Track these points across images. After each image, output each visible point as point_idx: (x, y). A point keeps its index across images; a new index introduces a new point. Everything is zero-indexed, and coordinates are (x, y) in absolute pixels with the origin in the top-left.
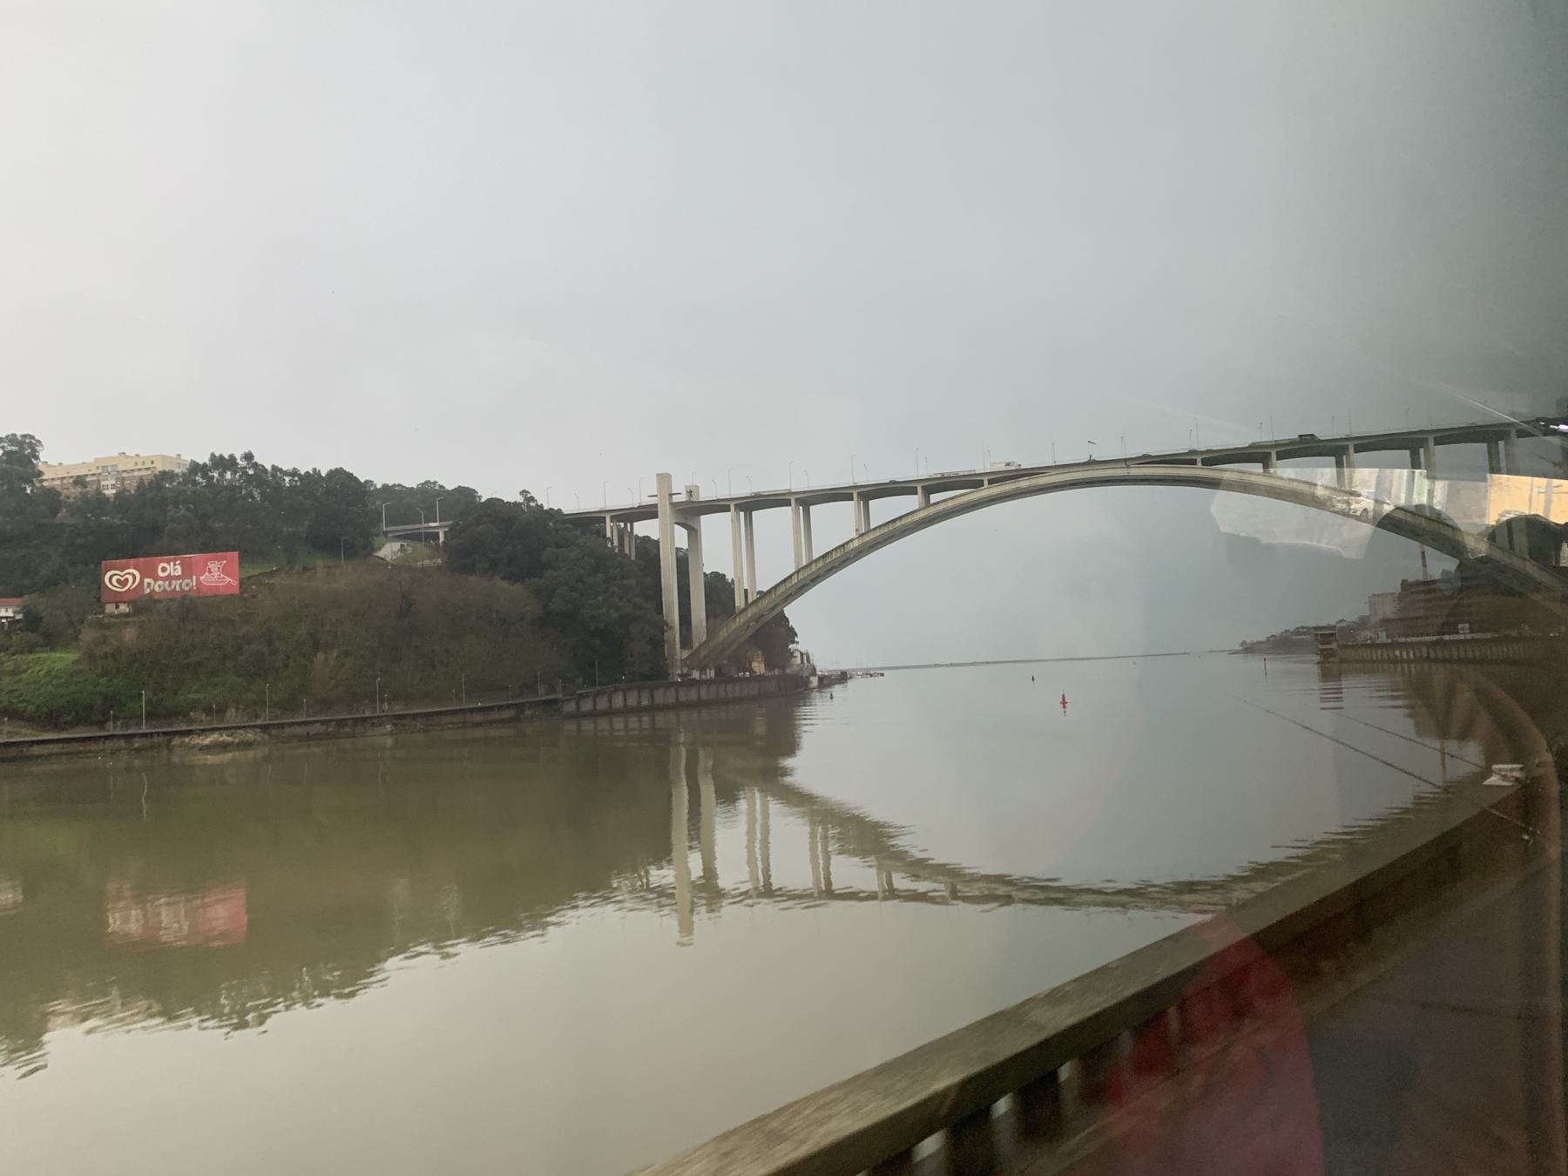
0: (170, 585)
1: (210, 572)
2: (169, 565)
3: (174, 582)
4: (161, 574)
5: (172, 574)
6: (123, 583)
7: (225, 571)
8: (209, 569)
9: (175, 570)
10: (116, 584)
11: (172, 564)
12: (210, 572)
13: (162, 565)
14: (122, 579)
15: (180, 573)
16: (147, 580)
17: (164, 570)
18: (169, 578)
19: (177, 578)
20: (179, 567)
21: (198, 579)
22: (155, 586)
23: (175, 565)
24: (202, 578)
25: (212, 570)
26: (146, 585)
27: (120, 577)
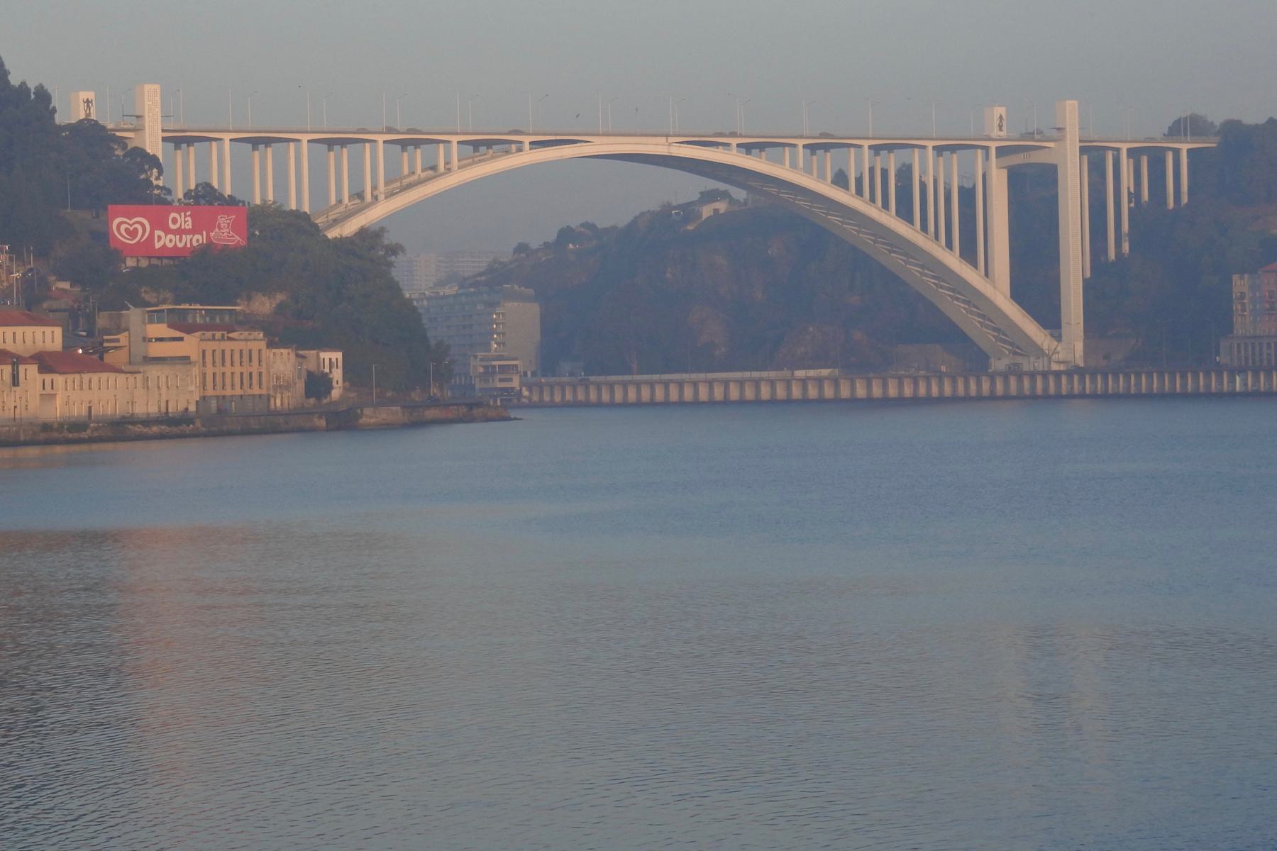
0: (181, 240)
1: (220, 228)
4: (172, 226)
5: (183, 227)
6: (133, 234)
7: (235, 227)
9: (185, 222)
10: (125, 234)
11: (183, 214)
12: (220, 228)
13: (173, 215)
14: (131, 229)
16: (157, 233)
18: (180, 232)
20: (189, 219)
21: (208, 237)
22: (164, 241)
23: (185, 216)
24: (212, 234)
27: (127, 226)
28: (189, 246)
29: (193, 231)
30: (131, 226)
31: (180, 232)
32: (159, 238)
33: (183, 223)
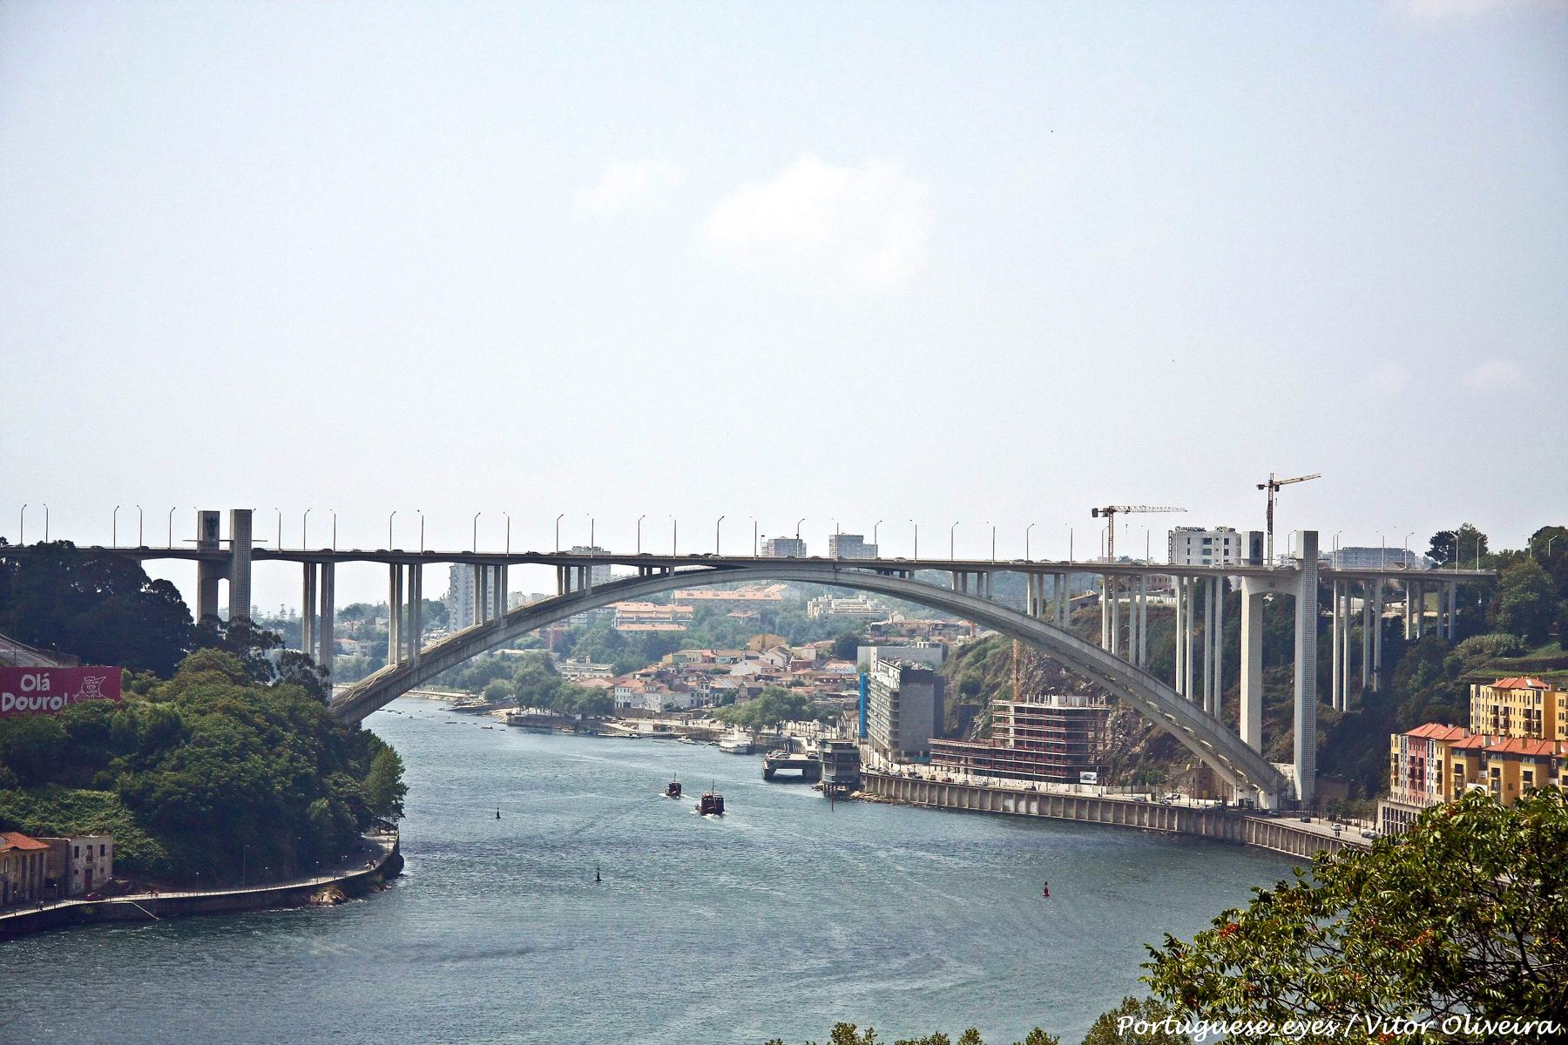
0: (35, 703)
1: (85, 689)
2: (35, 677)
3: (39, 699)
5: (39, 689)
8: (85, 686)
9: (42, 684)
11: (39, 676)
12: (85, 689)
13: (26, 677)
15: (48, 688)
17: (28, 683)
18: (35, 694)
20: (47, 680)
23: (42, 678)
26: (4, 701)
28: (45, 708)
31: (35, 694)
32: (8, 701)
33: (39, 685)
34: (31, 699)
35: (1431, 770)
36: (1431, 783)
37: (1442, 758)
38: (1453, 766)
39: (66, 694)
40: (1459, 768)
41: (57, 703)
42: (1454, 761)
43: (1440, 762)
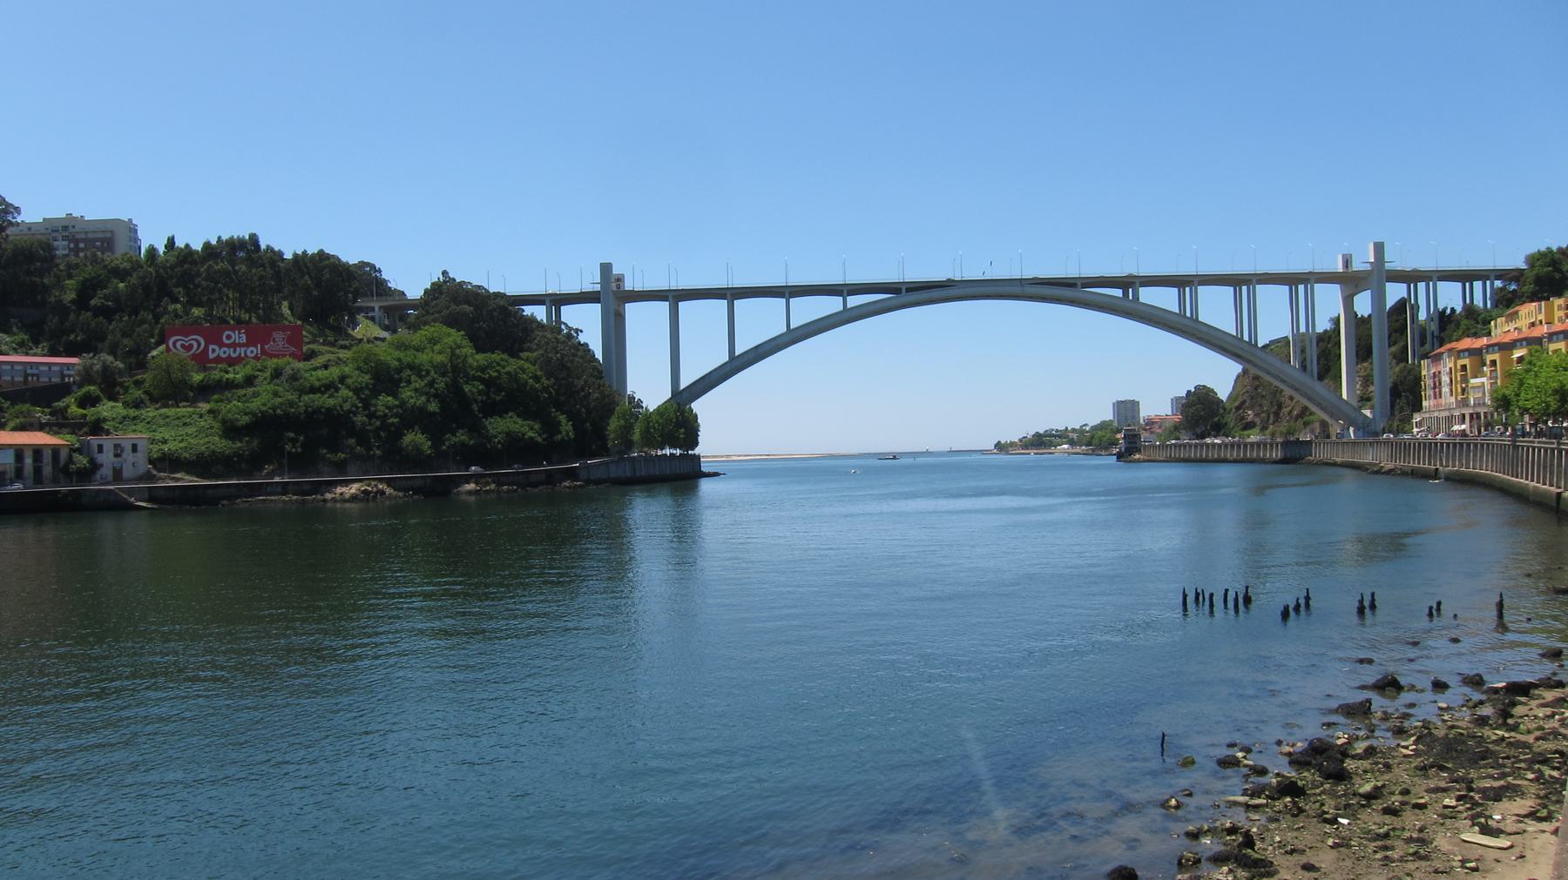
0: (235, 352)
1: (274, 341)
2: (234, 333)
3: (238, 349)
5: (237, 341)
8: (274, 339)
9: (240, 338)
11: (237, 332)
12: (274, 341)
13: (227, 333)
14: (187, 344)
15: (245, 341)
16: (211, 347)
17: (229, 337)
18: (234, 345)
19: (240, 345)
20: (244, 336)
23: (240, 333)
24: (266, 347)
25: (277, 340)
26: (210, 351)
28: (243, 355)
29: (247, 345)
30: (186, 342)
31: (234, 345)
32: (214, 351)
34: (232, 349)
35: (1445, 379)
36: (1445, 390)
37: (1452, 365)
38: (1459, 367)
39: (259, 346)
40: (1464, 367)
41: (252, 352)
42: (1461, 362)
43: (1451, 369)
